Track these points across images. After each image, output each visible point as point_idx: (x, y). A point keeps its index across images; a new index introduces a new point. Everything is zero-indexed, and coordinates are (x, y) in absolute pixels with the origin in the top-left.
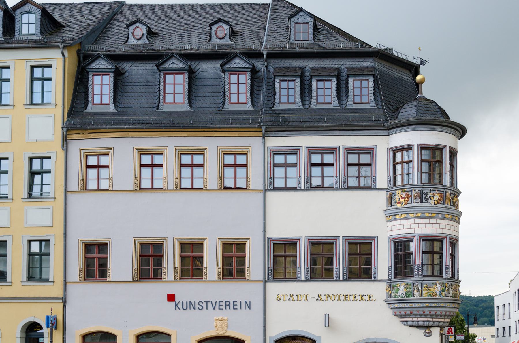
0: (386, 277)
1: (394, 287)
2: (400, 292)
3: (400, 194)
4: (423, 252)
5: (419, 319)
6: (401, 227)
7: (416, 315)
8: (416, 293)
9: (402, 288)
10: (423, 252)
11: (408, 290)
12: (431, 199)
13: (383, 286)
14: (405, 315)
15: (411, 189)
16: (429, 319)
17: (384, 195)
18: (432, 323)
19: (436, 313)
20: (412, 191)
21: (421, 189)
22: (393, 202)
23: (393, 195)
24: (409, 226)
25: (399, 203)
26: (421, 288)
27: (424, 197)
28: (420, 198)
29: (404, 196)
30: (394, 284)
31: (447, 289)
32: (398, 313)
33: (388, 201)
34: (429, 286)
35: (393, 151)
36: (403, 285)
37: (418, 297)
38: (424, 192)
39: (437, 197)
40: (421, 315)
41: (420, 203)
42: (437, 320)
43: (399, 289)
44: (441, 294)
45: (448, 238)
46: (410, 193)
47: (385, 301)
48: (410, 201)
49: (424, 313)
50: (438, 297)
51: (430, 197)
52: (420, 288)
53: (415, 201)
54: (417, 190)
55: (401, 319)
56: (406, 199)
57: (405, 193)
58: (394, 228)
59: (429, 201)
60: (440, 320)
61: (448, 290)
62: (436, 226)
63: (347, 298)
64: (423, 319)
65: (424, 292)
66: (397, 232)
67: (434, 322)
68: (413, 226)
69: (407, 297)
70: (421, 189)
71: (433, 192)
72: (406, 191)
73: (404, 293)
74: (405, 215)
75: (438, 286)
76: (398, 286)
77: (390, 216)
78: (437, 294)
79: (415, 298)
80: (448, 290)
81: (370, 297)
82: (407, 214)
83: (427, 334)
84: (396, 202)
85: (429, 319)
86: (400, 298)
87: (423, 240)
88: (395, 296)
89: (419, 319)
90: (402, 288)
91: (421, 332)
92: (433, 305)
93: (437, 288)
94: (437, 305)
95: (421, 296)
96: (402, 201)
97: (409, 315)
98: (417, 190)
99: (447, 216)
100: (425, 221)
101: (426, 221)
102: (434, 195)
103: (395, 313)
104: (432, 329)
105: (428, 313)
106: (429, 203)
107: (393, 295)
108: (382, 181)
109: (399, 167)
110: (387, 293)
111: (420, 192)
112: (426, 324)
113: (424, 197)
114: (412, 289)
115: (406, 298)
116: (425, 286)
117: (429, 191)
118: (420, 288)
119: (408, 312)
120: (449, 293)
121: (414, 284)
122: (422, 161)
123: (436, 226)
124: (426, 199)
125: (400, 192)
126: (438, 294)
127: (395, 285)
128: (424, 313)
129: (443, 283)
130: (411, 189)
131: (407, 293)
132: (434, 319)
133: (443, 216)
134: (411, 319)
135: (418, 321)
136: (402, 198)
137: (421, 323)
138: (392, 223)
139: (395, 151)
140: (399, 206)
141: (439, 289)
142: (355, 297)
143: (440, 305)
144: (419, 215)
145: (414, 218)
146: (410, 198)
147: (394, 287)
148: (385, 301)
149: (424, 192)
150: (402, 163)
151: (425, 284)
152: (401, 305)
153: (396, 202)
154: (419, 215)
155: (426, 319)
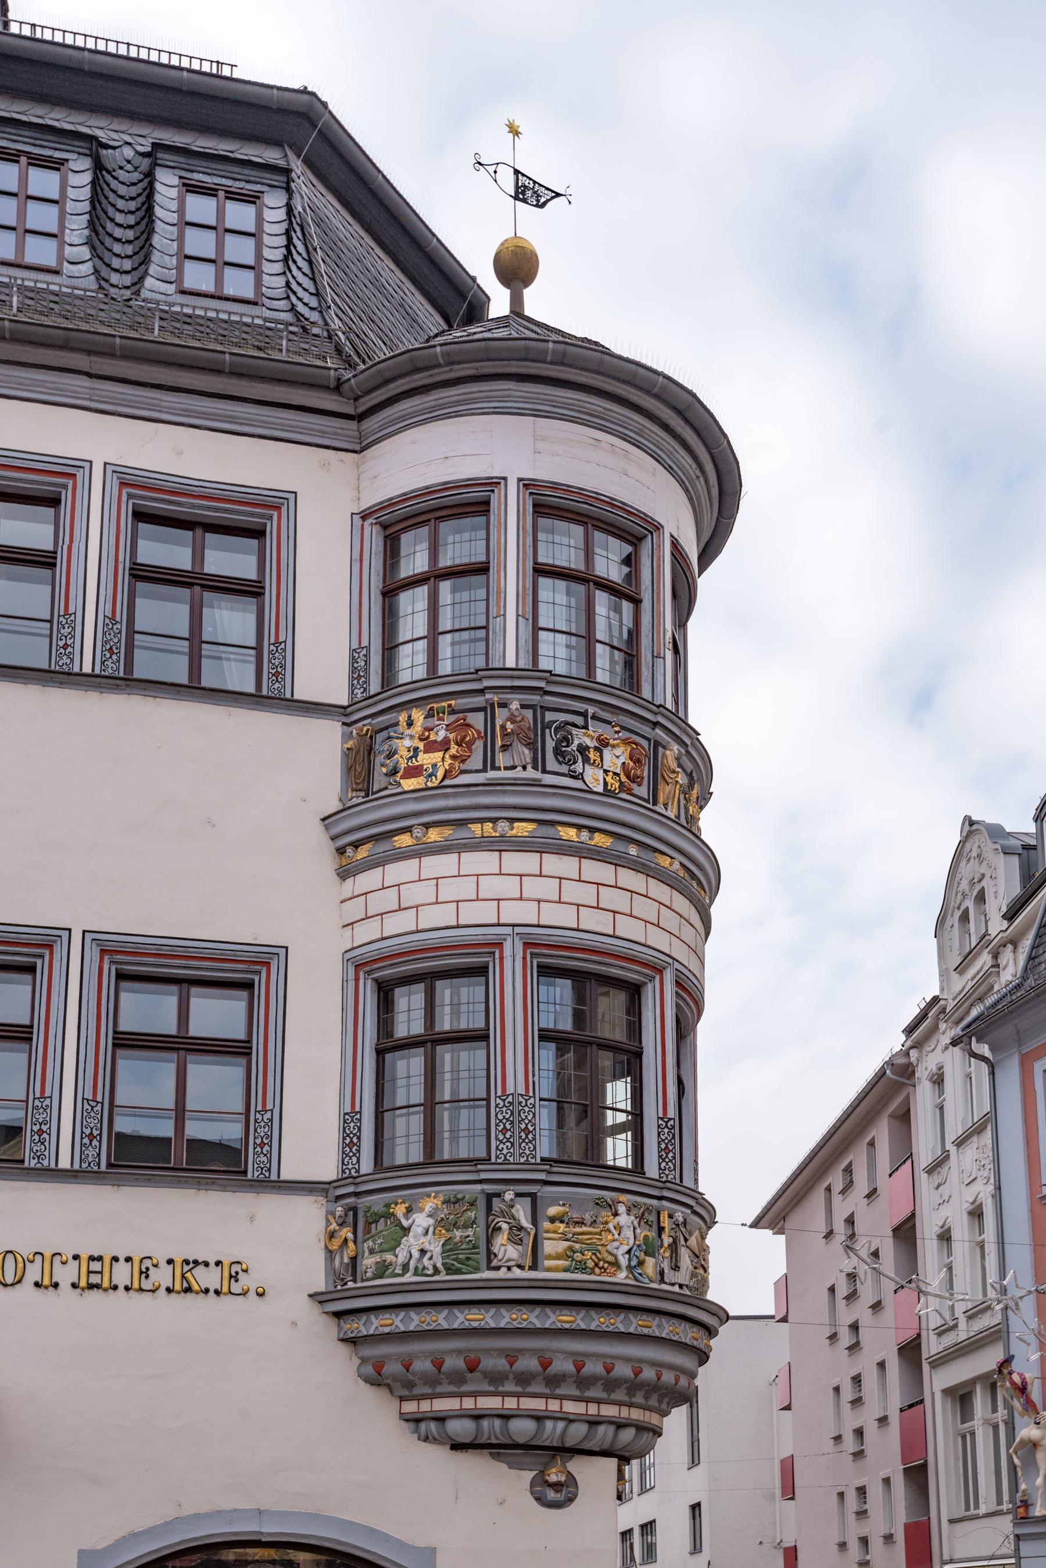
0: (327, 1169)
1: (373, 1219)
2: (412, 1243)
3: (418, 728)
4: (545, 1036)
5: (511, 1403)
6: (422, 893)
7: (496, 1378)
8: (505, 1249)
9: (421, 1221)
10: (545, 1036)
11: (458, 1234)
12: (586, 760)
13: (306, 1221)
14: (442, 1378)
15: (478, 701)
16: (570, 1407)
17: (325, 744)
18: (583, 1428)
19: (609, 1370)
20: (488, 710)
21: (535, 699)
22: (380, 772)
23: (380, 737)
24: (465, 888)
25: (413, 772)
26: (534, 1222)
27: (550, 744)
28: (531, 745)
29: (442, 734)
30: (375, 1202)
31: (667, 1240)
32: (393, 1368)
33: (349, 769)
34: (575, 1215)
35: (385, 527)
36: (429, 1205)
37: (517, 1273)
38: (549, 716)
39: (615, 758)
40: (524, 1379)
41: (531, 773)
42: (609, 1411)
43: (406, 1231)
44: (641, 1263)
45: (669, 976)
46: (477, 720)
47: (318, 1298)
48: (476, 761)
49: (545, 1364)
50: (621, 1276)
51: (583, 750)
52: (526, 1223)
53: (501, 759)
54: (515, 706)
55: (410, 1407)
56: (454, 750)
57: (448, 719)
58: (386, 900)
59: (579, 767)
60: (625, 1412)
61: (674, 1247)
62: (611, 898)
63: (95, 1277)
64: (536, 1404)
65: (549, 1247)
66: (400, 923)
67: (594, 1423)
68: (491, 886)
69: (449, 1270)
70: (535, 699)
71: (595, 729)
72: (453, 712)
73: (436, 1248)
74: (447, 832)
75: (624, 1219)
76: (400, 1210)
77: (357, 845)
78: (616, 1264)
79: (502, 1273)
80: (674, 1247)
81: (234, 1277)
82: (458, 828)
83: (551, 1495)
84: (394, 772)
85: (570, 1407)
86: (409, 1278)
87: (545, 971)
88: (383, 1269)
89: (511, 1403)
90: (421, 1221)
91: (516, 1482)
92: (599, 1321)
93: (619, 1228)
94: (618, 1323)
95: (534, 1267)
96: (425, 759)
97: (457, 1378)
98: (515, 706)
99: (665, 861)
100: (554, 864)
101: (567, 865)
102: (603, 743)
103: (378, 1367)
104: (578, 1466)
105: (569, 1367)
106: (579, 777)
107: (369, 1262)
108: (322, 665)
109: (413, 606)
110: (330, 1253)
111: (529, 714)
112: (552, 1430)
113: (550, 744)
114: (480, 1229)
115: (443, 1277)
116: (553, 1211)
117: (579, 720)
118: (526, 1223)
119: (454, 1363)
120: (676, 1268)
121: (490, 1197)
122: (541, 571)
123: (611, 898)
124: (558, 752)
125: (418, 715)
126: (623, 1261)
127: (379, 1208)
128: (545, 1364)
129: (648, 1209)
130: (478, 701)
131: (449, 1248)
132: (593, 1409)
133: (648, 855)
134: (468, 1403)
135: (506, 1417)
136: (431, 747)
137: (522, 1429)
138: (368, 880)
139: (393, 523)
140: (409, 784)
141: (628, 1233)
142: (145, 1273)
143: (635, 1324)
144: (523, 829)
145: (501, 845)
146: (479, 745)
147: (373, 1219)
148: (318, 1298)
149: (549, 716)
150: (433, 577)
151: (554, 1201)
152: (415, 1321)
153: (394, 772)
154: (523, 829)
155: (554, 1405)
